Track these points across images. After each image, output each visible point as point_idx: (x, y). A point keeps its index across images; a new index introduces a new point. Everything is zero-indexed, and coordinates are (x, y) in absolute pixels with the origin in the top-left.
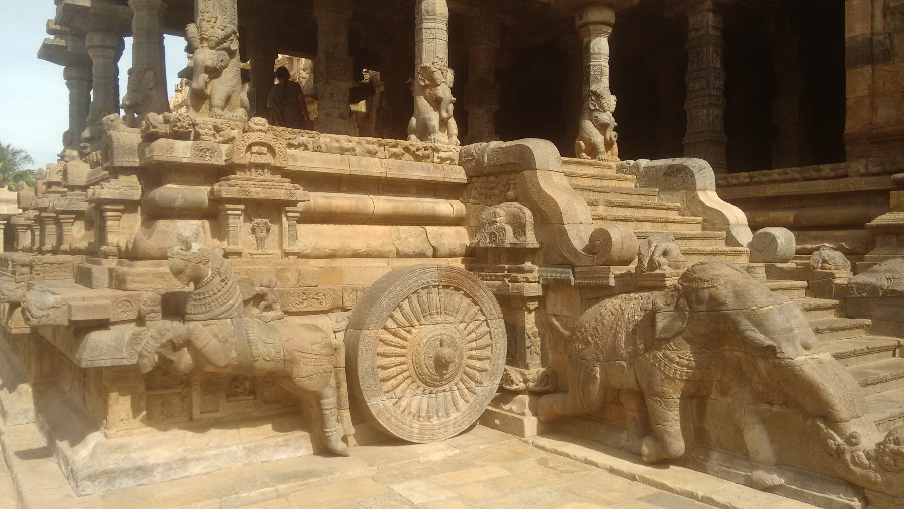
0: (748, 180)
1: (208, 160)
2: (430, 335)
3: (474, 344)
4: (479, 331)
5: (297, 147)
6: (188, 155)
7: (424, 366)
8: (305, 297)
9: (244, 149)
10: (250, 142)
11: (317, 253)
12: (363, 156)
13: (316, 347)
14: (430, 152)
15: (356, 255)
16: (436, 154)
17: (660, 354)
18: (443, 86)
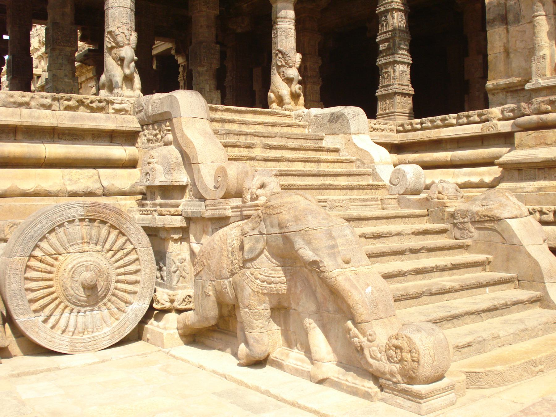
0: (419, 126)
2: (75, 262)
3: (122, 270)
4: (127, 259)
7: (70, 289)
12: (38, 109)
14: (104, 104)
15: (25, 195)
16: (111, 107)
17: (248, 272)
18: (126, 47)
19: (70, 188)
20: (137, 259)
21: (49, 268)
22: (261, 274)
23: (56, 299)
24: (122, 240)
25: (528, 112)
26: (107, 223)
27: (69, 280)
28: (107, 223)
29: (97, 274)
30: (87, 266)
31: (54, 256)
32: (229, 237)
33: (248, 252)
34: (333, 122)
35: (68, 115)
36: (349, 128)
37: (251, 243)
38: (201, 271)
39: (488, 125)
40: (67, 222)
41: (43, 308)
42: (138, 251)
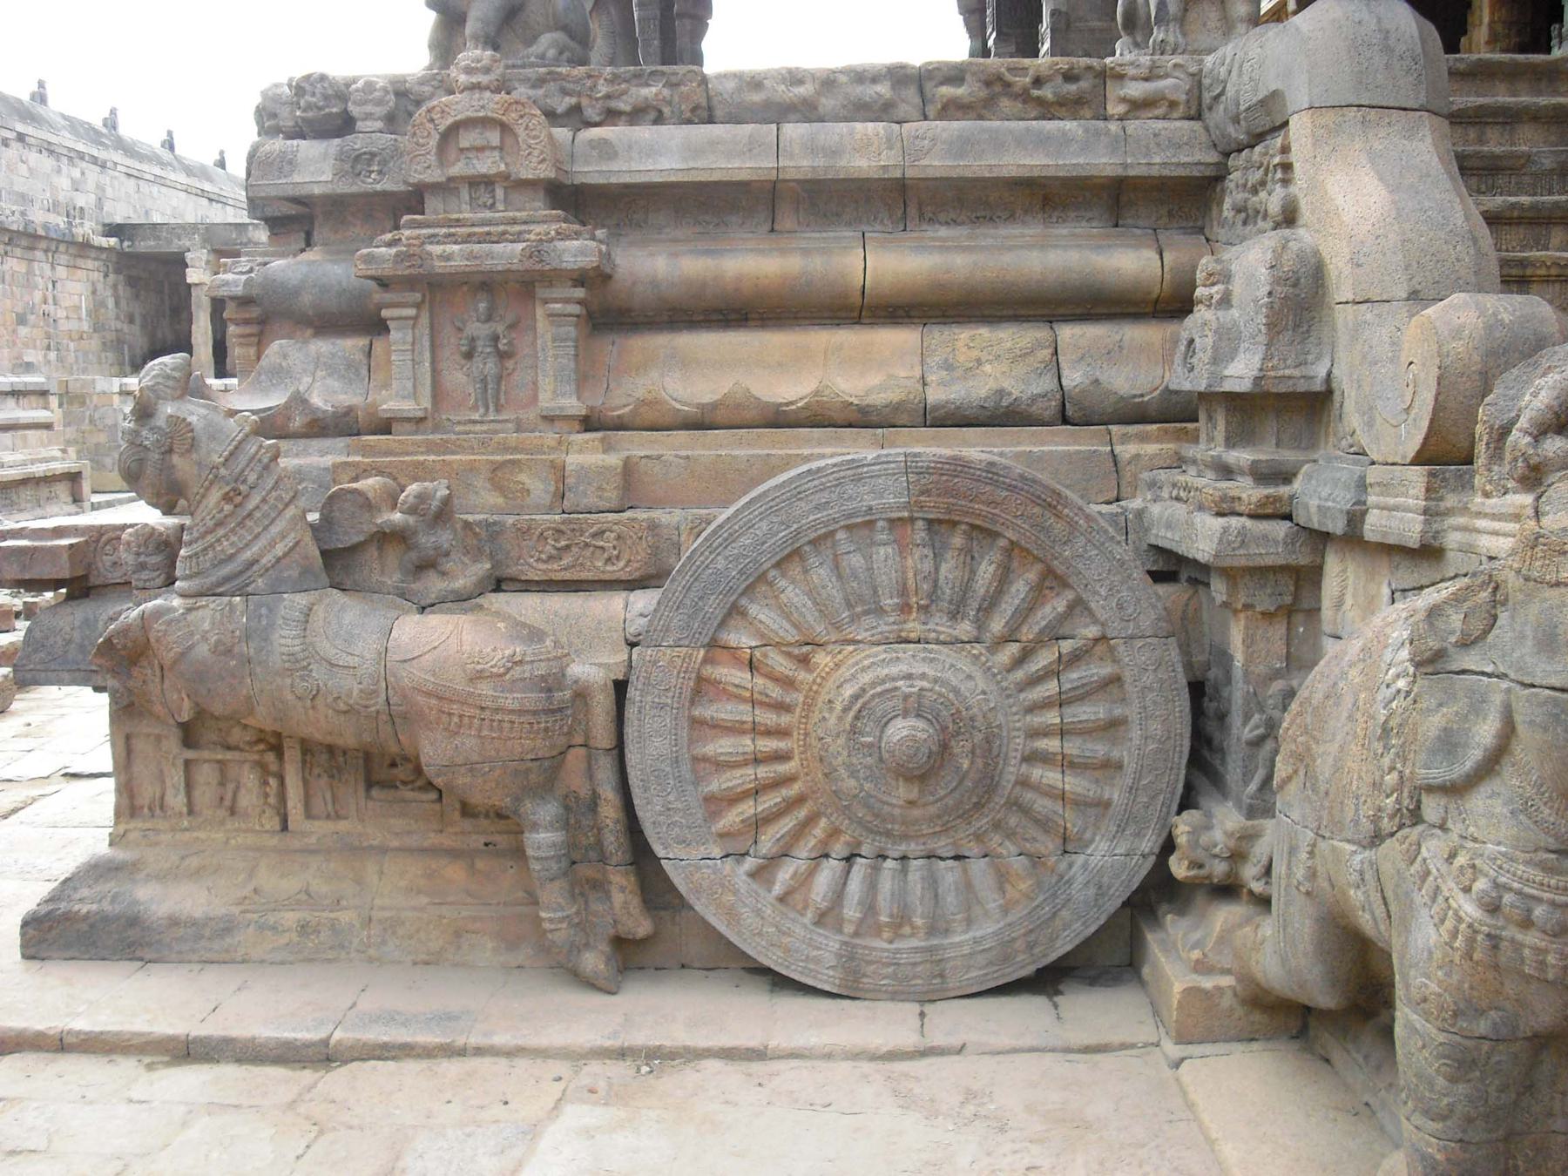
1: (375, 183)
2: (866, 678)
3: (1052, 717)
4: (1073, 676)
5: (636, 115)
6: (327, 177)
7: (843, 772)
8: (563, 543)
9: (433, 142)
10: (450, 121)
11: (649, 416)
12: (846, 120)
13: (485, 689)
19: (935, 395)
20: (1116, 680)
21: (776, 692)
23: (800, 800)
24: (1059, 604)
26: (995, 535)
27: (841, 741)
28: (995, 535)
29: (944, 729)
30: (906, 697)
31: (796, 651)
35: (945, 135)
40: (848, 528)
41: (759, 823)
42: (1121, 649)
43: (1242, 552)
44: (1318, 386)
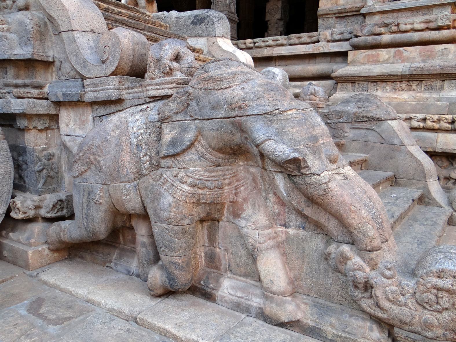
0: (252, 45)
22: (189, 177)
25: (360, 34)
32: (131, 125)
33: (169, 146)
34: (196, 24)
36: (214, 30)
37: (173, 133)
38: (86, 171)
39: (319, 45)
43: (35, 109)
44: (51, 60)
